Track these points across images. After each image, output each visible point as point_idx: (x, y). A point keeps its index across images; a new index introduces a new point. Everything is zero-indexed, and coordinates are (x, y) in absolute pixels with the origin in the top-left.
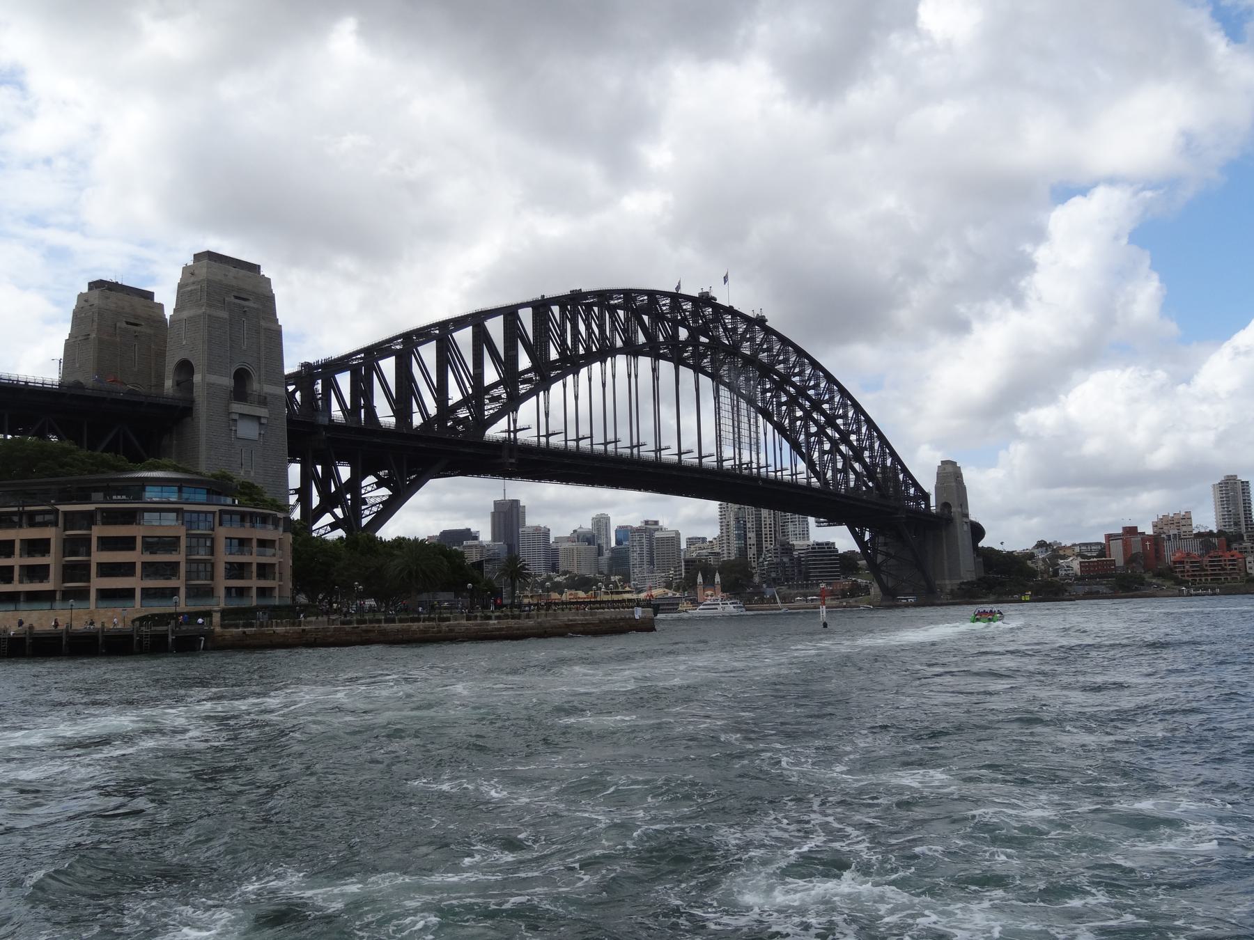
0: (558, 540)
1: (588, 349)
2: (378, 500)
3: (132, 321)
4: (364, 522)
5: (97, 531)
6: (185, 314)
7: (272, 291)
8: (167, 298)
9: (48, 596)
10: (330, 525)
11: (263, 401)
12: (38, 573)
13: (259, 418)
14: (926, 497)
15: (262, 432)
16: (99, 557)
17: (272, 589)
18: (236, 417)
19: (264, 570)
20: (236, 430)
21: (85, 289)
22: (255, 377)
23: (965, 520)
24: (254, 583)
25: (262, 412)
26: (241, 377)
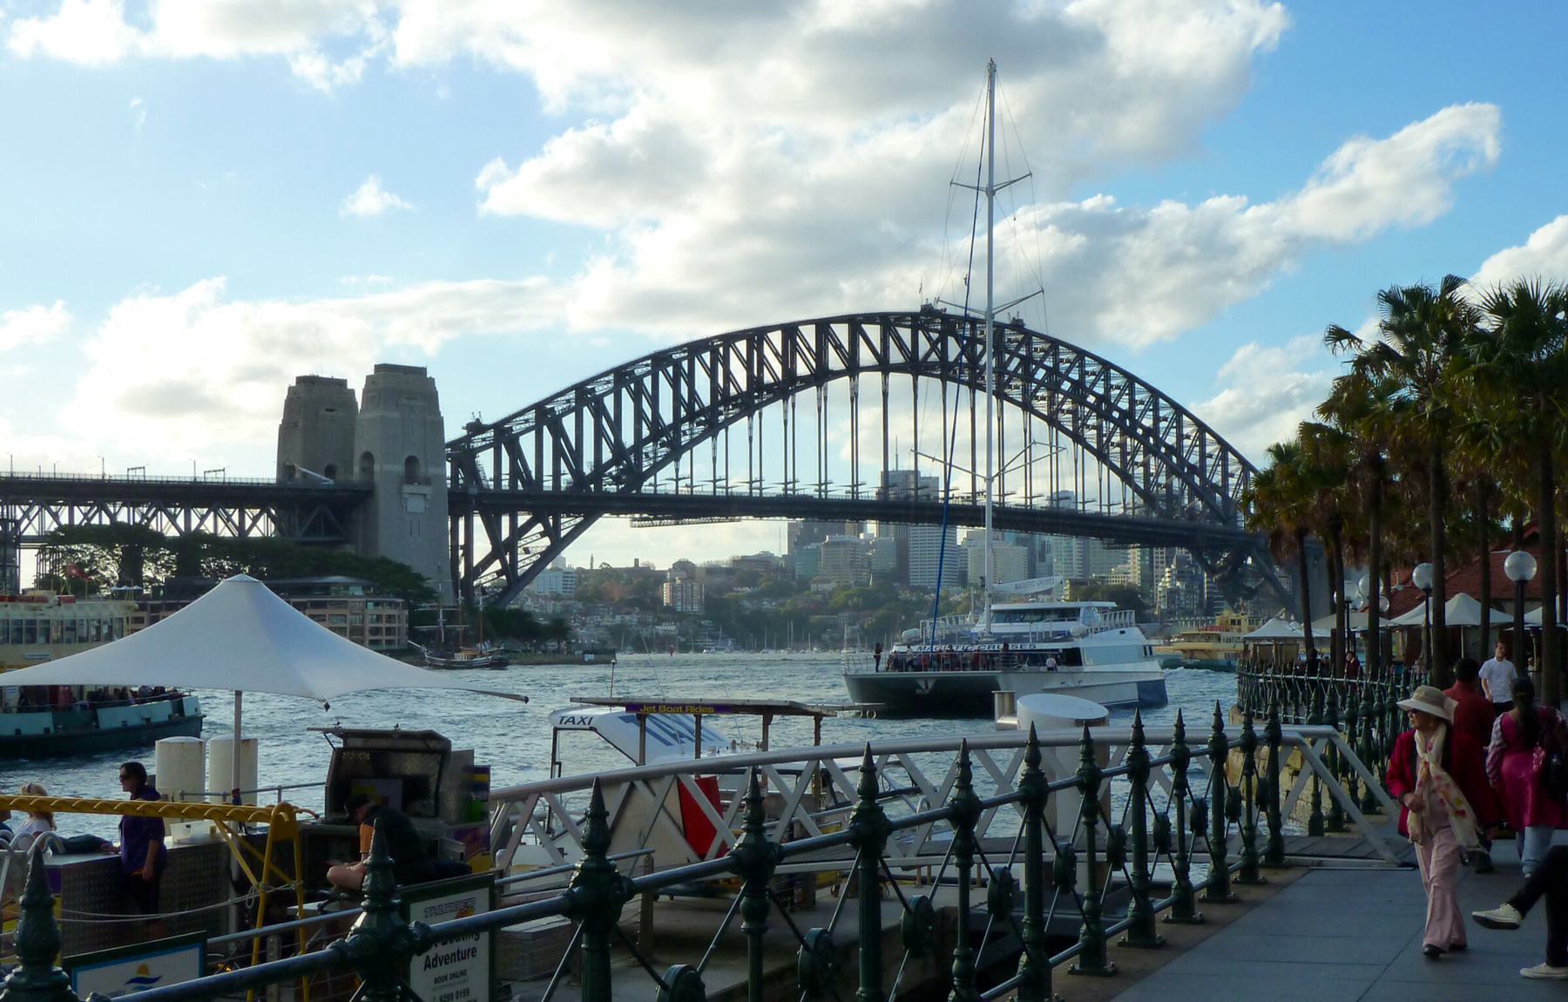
2: (539, 550)
3: (330, 407)
6: (368, 415)
7: (435, 388)
8: (357, 385)
10: (497, 572)
11: (427, 481)
13: (425, 495)
15: (427, 506)
17: (394, 640)
18: (405, 496)
19: (389, 631)
20: (406, 507)
21: (294, 384)
22: (421, 461)
24: (384, 638)
25: (427, 490)
26: (411, 461)
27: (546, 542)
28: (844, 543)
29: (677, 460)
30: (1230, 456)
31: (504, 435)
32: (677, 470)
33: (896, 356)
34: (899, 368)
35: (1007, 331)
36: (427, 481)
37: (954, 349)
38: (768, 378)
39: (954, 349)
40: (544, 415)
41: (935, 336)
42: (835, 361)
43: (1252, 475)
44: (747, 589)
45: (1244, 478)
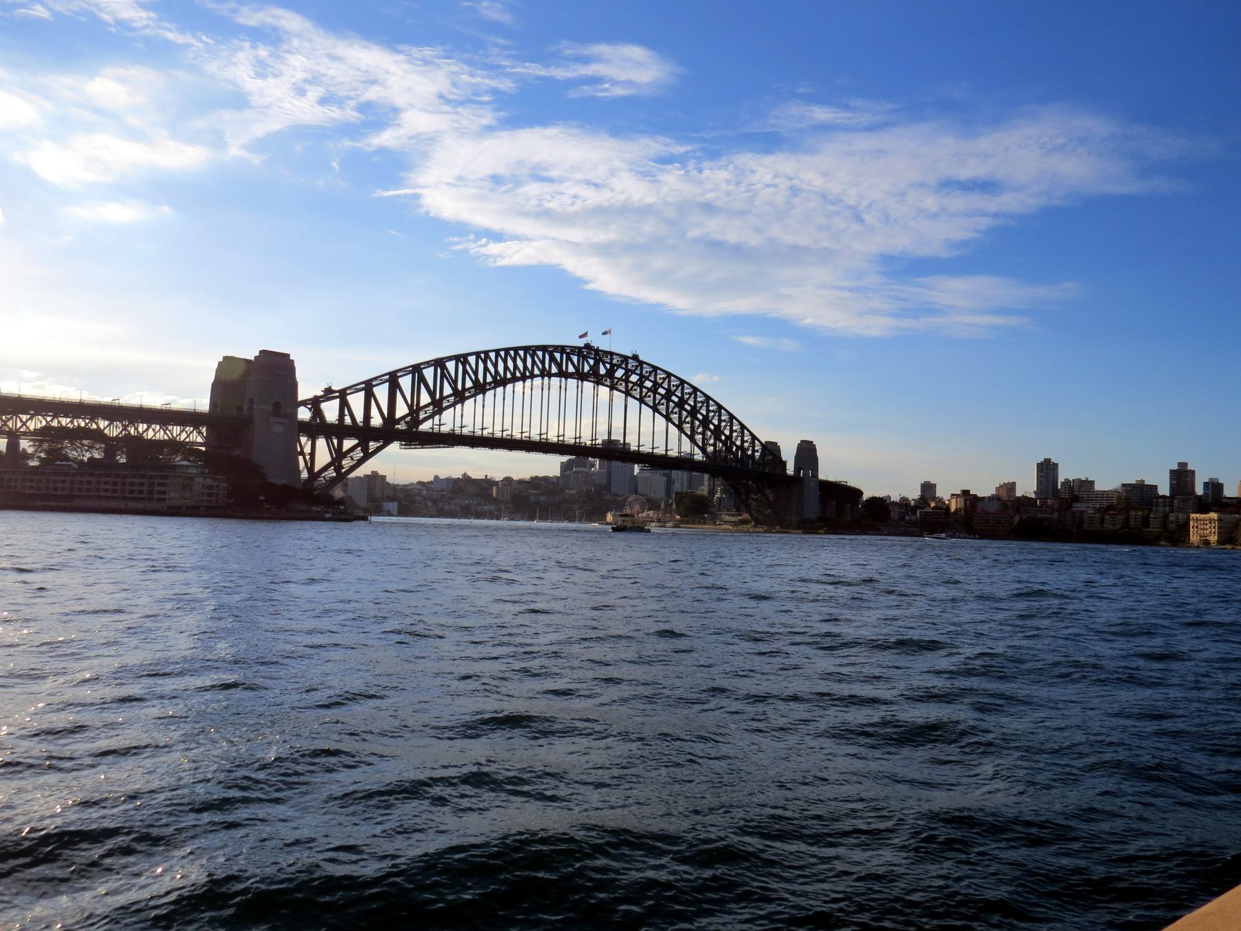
1: (513, 374)
4: (343, 471)
5: (157, 481)
9: (143, 499)
11: (286, 416)
12: (141, 492)
14: (784, 464)
16: (157, 488)
23: (814, 479)
25: (285, 421)
26: (277, 405)
27: (362, 454)
29: (440, 414)
30: (746, 431)
31: (343, 395)
32: (440, 420)
33: (571, 369)
34: (570, 376)
35: (630, 361)
36: (286, 416)
37: (602, 371)
38: (498, 378)
39: (602, 371)
40: (368, 387)
41: (592, 362)
42: (536, 372)
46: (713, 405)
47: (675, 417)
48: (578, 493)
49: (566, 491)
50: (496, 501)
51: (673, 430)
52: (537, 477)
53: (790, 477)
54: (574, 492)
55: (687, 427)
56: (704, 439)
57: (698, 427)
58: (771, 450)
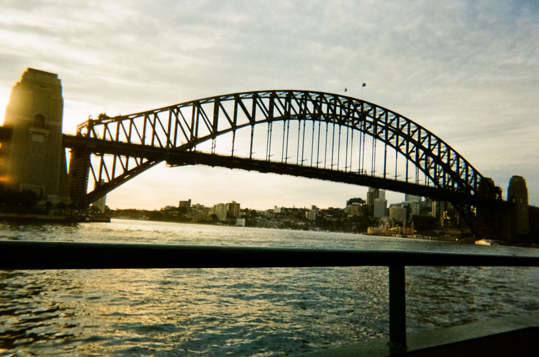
0: (391, 205)
11: (48, 128)
13: (44, 134)
25: (47, 132)
28: (357, 205)
36: (48, 128)
43: (478, 176)
44: (330, 215)
45: (475, 177)
46: (444, 147)
47: (413, 155)
48: (355, 216)
49: (348, 216)
50: (306, 220)
51: (412, 166)
52: (332, 208)
53: (504, 202)
54: (352, 216)
55: (422, 163)
56: (435, 172)
57: (432, 163)
58: (487, 183)
